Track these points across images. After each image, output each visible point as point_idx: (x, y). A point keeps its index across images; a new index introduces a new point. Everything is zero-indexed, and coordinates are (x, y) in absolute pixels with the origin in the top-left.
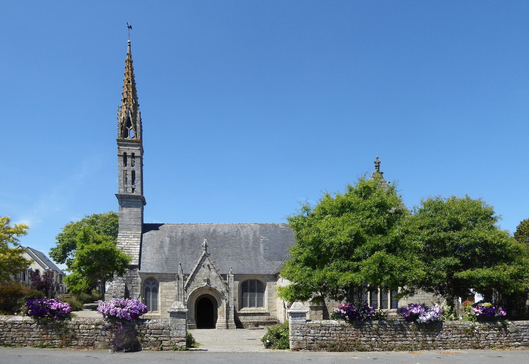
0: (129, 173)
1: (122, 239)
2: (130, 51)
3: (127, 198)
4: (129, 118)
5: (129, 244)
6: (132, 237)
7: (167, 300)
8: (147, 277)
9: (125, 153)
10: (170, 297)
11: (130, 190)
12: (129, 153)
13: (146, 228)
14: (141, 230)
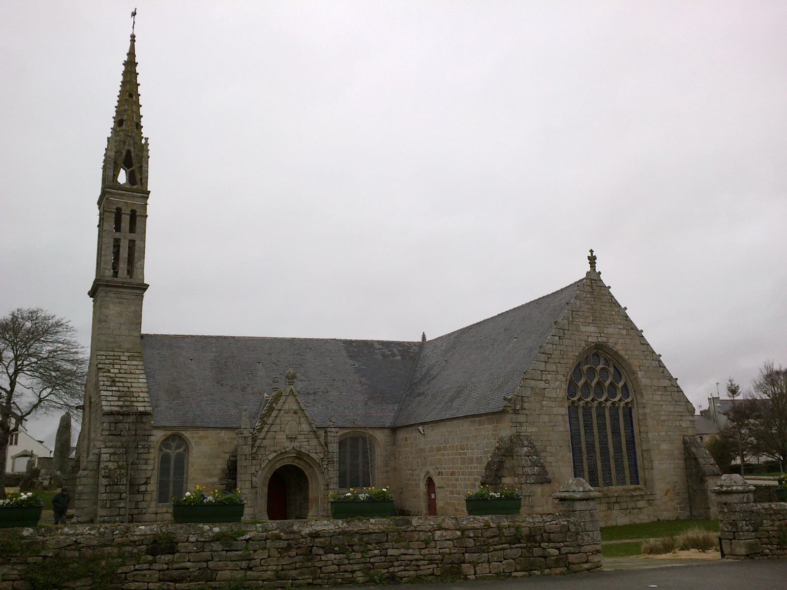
3: (118, 287)
6: (126, 358)
8: (169, 433)
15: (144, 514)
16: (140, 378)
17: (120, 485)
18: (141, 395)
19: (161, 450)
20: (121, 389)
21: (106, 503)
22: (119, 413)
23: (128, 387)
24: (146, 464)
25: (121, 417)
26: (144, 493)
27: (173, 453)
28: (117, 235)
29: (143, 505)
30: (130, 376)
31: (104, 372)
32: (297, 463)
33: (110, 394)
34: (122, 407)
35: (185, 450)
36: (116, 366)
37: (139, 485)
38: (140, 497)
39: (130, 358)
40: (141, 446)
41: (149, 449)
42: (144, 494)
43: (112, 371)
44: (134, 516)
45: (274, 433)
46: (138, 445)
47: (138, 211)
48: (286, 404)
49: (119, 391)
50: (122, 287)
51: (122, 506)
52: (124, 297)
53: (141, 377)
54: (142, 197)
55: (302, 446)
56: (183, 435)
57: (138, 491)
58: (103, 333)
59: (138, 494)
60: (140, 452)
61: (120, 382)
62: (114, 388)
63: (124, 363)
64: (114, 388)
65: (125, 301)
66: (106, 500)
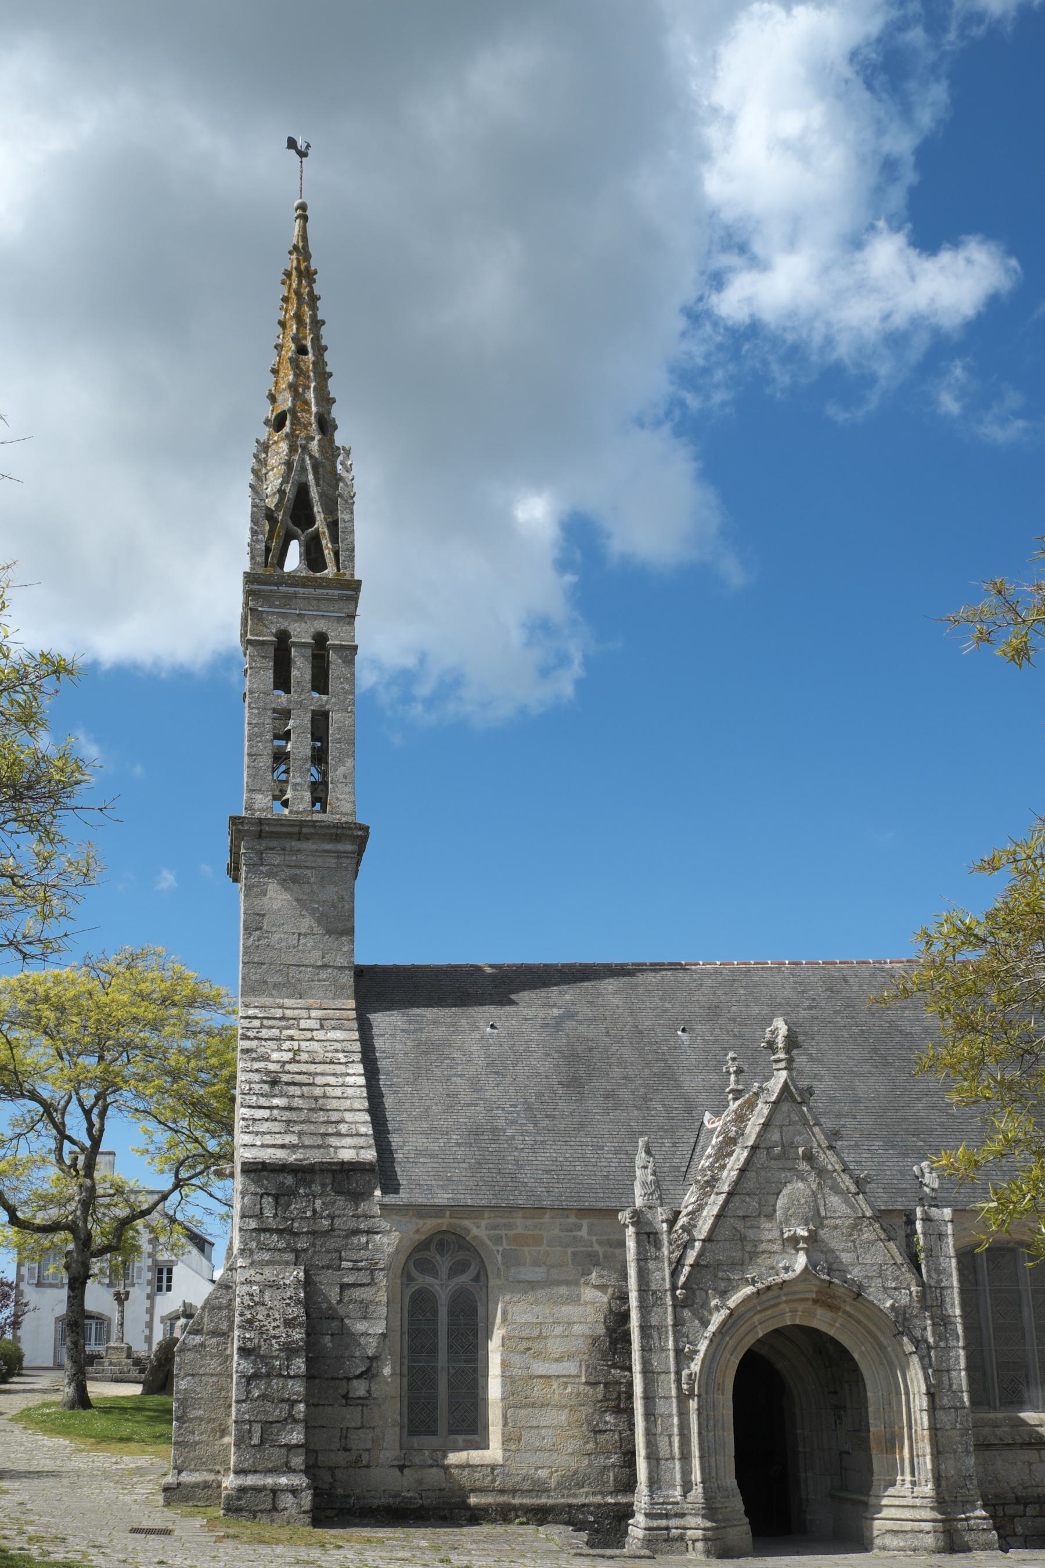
0: (299, 723)
1: (265, 1033)
2: (304, 236)
3: (289, 836)
4: (302, 490)
5: (304, 1057)
7: (540, 1368)
8: (430, 1225)
9: (283, 637)
10: (555, 1347)
11: (300, 799)
12: (301, 633)
13: (379, 988)
14: (351, 991)
15: (368, 1467)
16: (348, 1075)
17: (289, 1377)
18: (348, 1116)
19: (407, 1277)
20: (298, 1102)
21: (250, 1431)
22: (283, 1168)
23: (316, 1099)
24: (365, 1318)
25: (289, 1180)
26: (363, 1402)
27: (442, 1289)
28: (282, 698)
29: (359, 1441)
30: (320, 1068)
31: (253, 1059)
32: (821, 1321)
33: (266, 1113)
34: (293, 1147)
35: (476, 1279)
36: (287, 1045)
37: (349, 1379)
38: (352, 1416)
39: (326, 1023)
40: (350, 1264)
41: (372, 1272)
42: (363, 1405)
43: (275, 1056)
44: (337, 1472)
45: (740, 1225)
46: (341, 1259)
47: (331, 634)
48: (770, 1129)
49: (289, 1108)
50: (300, 836)
51: (294, 1442)
52: (306, 864)
53: (350, 1071)
54: (341, 598)
55: (835, 1266)
56: (468, 1231)
57: (346, 1397)
58: (256, 960)
59: (347, 1405)
60: (345, 1280)
61: (294, 1084)
62: (276, 1101)
63: (309, 1035)
64: (276, 1101)
65: (308, 872)
66: (250, 1422)
